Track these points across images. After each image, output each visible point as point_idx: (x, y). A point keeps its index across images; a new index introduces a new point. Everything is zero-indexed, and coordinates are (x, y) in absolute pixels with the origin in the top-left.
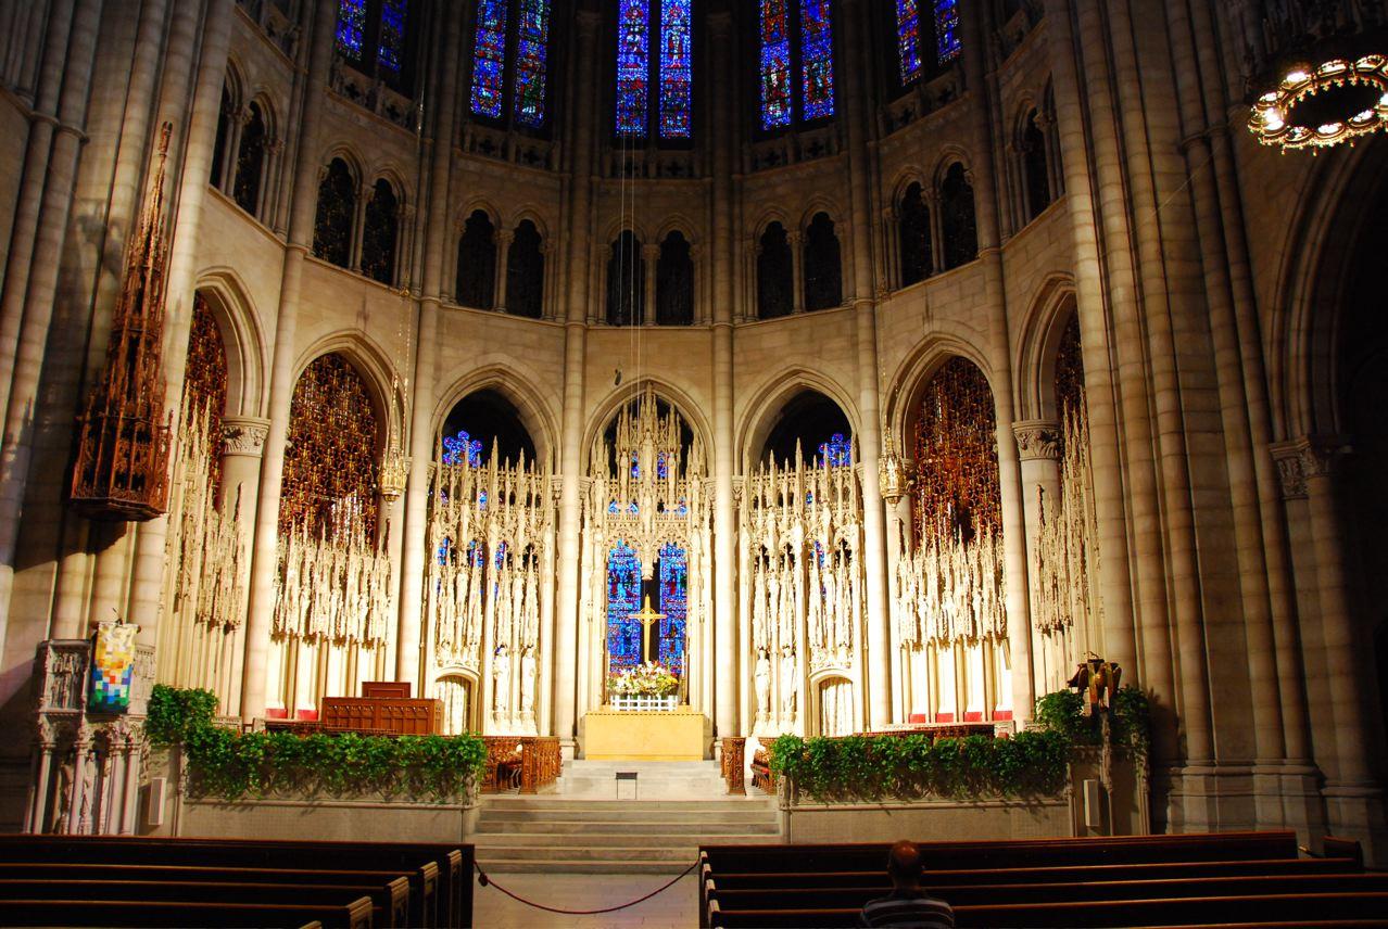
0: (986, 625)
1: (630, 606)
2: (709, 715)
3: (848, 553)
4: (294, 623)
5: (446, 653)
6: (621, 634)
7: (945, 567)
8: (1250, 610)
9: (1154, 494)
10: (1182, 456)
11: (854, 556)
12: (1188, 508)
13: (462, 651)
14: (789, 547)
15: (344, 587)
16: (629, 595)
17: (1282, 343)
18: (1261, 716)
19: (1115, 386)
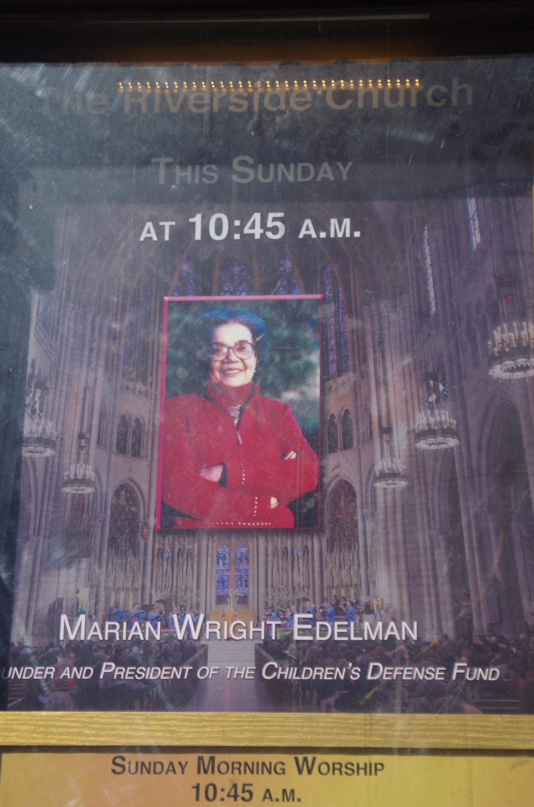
0: (355, 581)
1: (224, 568)
2: (256, 613)
3: (308, 551)
4: (111, 585)
5: (159, 591)
6: (221, 580)
7: (342, 559)
8: (424, 582)
9: (396, 543)
10: (404, 532)
11: (310, 553)
12: (406, 549)
13: (164, 591)
14: (286, 548)
15: (126, 570)
16: (224, 563)
17: (433, 499)
18: (427, 615)
19: (386, 508)
